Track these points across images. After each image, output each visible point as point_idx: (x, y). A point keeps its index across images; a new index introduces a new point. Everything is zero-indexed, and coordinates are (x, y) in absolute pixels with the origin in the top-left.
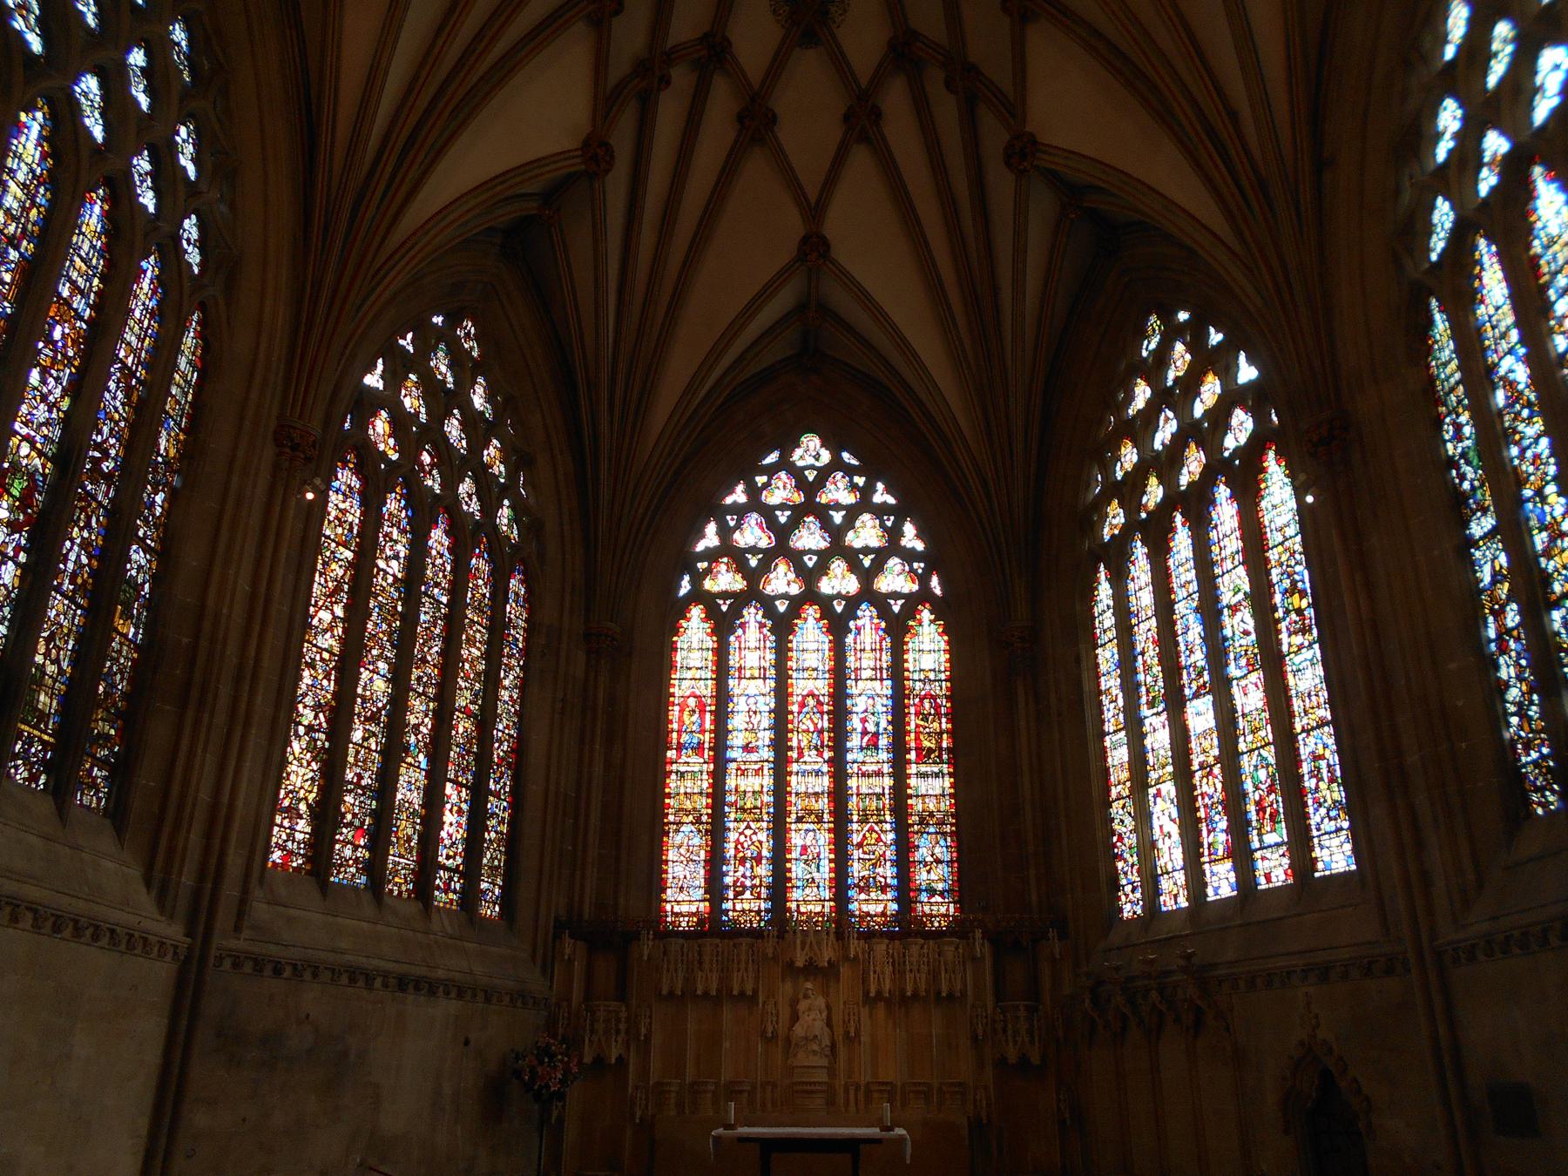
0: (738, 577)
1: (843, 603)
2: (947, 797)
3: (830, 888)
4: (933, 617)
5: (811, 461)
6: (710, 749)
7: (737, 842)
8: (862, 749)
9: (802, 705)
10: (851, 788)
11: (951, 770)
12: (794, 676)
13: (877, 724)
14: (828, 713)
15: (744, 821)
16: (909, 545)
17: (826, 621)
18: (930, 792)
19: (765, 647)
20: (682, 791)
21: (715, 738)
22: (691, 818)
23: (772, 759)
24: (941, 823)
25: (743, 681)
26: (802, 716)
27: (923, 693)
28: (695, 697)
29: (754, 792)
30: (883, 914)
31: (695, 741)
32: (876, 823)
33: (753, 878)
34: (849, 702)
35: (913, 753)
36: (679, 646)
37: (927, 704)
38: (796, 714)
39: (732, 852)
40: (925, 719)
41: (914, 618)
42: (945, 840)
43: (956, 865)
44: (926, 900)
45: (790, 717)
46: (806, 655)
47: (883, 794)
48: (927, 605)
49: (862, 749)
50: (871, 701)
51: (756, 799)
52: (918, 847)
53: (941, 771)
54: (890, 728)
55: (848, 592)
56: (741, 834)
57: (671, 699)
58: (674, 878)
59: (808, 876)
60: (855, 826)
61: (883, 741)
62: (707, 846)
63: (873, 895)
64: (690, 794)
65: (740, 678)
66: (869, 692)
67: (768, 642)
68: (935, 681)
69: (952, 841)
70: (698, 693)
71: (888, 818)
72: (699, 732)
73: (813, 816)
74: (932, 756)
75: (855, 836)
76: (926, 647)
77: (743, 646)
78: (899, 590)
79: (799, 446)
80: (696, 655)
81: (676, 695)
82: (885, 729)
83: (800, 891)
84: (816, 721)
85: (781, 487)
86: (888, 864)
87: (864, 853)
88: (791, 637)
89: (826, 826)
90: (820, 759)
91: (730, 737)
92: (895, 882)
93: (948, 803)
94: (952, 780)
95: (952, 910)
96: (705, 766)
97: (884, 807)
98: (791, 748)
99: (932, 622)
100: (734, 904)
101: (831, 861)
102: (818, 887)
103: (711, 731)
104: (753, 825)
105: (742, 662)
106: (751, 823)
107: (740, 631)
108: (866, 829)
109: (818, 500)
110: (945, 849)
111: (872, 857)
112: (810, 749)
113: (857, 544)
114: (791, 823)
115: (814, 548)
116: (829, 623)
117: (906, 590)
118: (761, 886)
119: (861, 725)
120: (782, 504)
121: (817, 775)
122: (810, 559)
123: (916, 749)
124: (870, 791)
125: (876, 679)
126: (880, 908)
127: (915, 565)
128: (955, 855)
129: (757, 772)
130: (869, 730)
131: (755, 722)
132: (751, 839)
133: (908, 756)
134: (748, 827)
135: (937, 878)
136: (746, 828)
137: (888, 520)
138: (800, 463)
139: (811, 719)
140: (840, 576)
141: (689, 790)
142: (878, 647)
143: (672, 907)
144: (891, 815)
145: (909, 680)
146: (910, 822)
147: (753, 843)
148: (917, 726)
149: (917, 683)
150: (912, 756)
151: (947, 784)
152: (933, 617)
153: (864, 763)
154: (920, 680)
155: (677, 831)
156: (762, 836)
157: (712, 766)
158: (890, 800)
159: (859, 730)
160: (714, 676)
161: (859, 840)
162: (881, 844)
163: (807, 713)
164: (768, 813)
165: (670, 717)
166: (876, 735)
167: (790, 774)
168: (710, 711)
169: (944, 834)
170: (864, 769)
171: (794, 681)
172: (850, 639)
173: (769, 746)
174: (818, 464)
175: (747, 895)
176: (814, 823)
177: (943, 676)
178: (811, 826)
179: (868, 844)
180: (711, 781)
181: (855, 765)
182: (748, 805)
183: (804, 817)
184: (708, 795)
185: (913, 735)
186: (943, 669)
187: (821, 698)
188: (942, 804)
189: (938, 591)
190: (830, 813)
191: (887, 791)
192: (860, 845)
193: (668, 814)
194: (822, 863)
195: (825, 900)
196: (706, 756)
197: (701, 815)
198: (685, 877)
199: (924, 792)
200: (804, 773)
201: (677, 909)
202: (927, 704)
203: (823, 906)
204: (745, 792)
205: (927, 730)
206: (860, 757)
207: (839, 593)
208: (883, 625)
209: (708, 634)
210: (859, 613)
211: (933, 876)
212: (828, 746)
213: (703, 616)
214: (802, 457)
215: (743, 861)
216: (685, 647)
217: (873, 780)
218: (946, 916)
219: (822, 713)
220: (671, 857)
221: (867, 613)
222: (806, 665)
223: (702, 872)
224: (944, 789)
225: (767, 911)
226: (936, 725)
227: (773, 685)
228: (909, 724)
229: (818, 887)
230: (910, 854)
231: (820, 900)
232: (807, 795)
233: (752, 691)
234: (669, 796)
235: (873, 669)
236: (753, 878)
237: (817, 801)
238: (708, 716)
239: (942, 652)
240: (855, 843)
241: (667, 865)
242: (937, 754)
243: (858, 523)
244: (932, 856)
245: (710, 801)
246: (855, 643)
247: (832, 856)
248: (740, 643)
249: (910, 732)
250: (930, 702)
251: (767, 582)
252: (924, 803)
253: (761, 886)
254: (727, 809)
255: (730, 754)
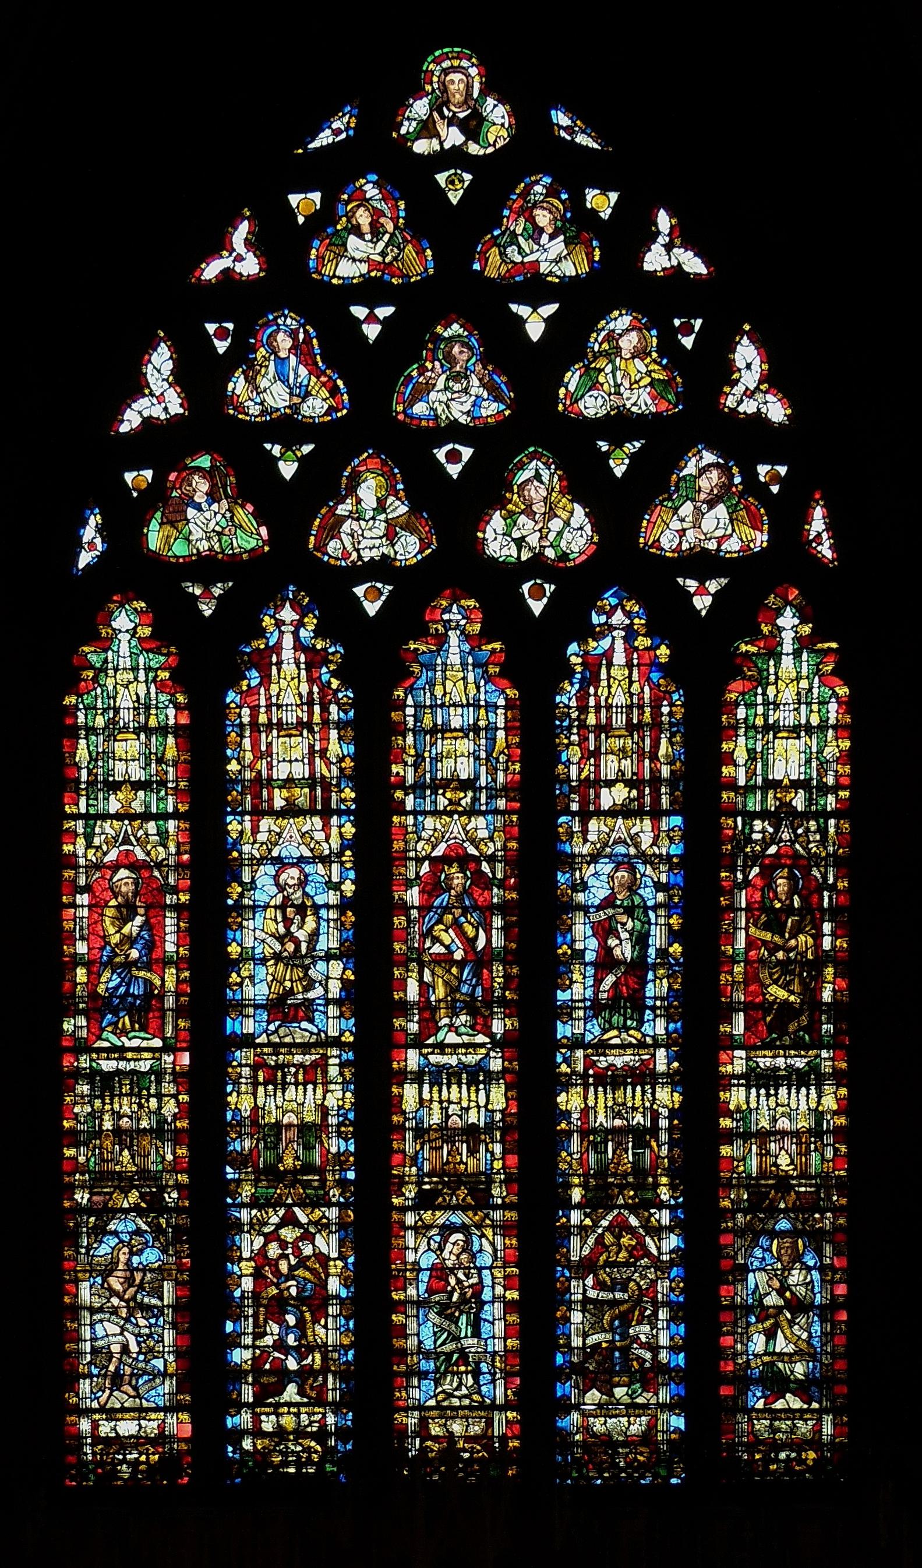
0: (244, 515)
1: (550, 588)
2: (829, 1139)
3: (507, 1376)
4: (806, 630)
5: (454, 137)
6: (179, 1012)
7: (261, 1257)
8: (596, 1008)
9: (433, 887)
10: (568, 1113)
11: (844, 1065)
12: (409, 806)
13: (641, 940)
14: (503, 908)
15: (278, 1203)
16: (749, 407)
17: (497, 646)
18: (783, 1124)
19: (325, 723)
20: (108, 1125)
21: (191, 981)
22: (134, 1197)
23: (348, 1038)
24: (807, 1206)
25: (265, 823)
26: (431, 917)
27: (773, 850)
28: (134, 866)
29: (304, 1128)
30: (647, 1437)
31: (137, 990)
32: (633, 1209)
33: (303, 1350)
34: (562, 878)
35: (740, 1019)
36: (81, 718)
37: (782, 885)
38: (415, 913)
39: (248, 1284)
40: (775, 924)
41: (754, 635)
42: (819, 1253)
43: (844, 1316)
44: (760, 1405)
45: (399, 921)
46: (443, 746)
47: (654, 1130)
48: (793, 594)
49: (596, 1008)
50: (622, 874)
51: (308, 1148)
52: (745, 1270)
53: (813, 1068)
54: (676, 948)
55: (564, 557)
56: (269, 1238)
57: (68, 874)
58: (95, 1351)
59: (449, 1347)
60: (575, 1217)
61: (656, 988)
62: (181, 1269)
63: (619, 1392)
64: (129, 1132)
65: (257, 813)
66: (621, 849)
67: (333, 708)
68: (806, 815)
69: (836, 1253)
70: (140, 854)
71: (665, 1194)
72: (148, 967)
73: (462, 1192)
74: (791, 1028)
75: (575, 1242)
76: (786, 717)
77: (263, 719)
78: (712, 545)
79: (418, 93)
80: (129, 746)
81: (82, 861)
82: (662, 953)
83: (428, 1385)
84: (470, 931)
85: (366, 228)
86: (662, 1314)
87: (599, 1285)
88: (400, 693)
89: (497, 1215)
90: (481, 1039)
91: (234, 977)
92: (681, 1359)
93: (829, 1153)
94: (843, 1091)
95: (827, 1429)
96: (169, 1059)
97: (655, 1166)
98: (404, 1008)
99: (803, 644)
100: (256, 1419)
101: (509, 1306)
102: (477, 1373)
103: (178, 963)
104: (302, 1216)
105: (262, 765)
106: (296, 1210)
107: (254, 677)
108: (605, 1223)
109: (477, 266)
110: (816, 1275)
111: (618, 1295)
112: (454, 1013)
113: (592, 406)
114: (403, 1209)
115: (463, 419)
116: (508, 651)
117: (733, 546)
118: (325, 1370)
119: (593, 943)
120: (367, 281)
121: (473, 1082)
122: (454, 457)
123: (747, 1008)
124: (618, 1122)
125: (640, 813)
126: (638, 1426)
127: (763, 470)
128: (841, 1290)
129: (315, 1073)
130: (617, 952)
131: (301, 935)
132: (297, 1252)
133: (725, 1028)
134: (289, 1220)
135: (790, 1349)
136: (283, 1223)
137: (687, 330)
138: (421, 147)
139: (457, 926)
140: (539, 508)
141: (125, 1122)
142: (647, 717)
143: (95, 1425)
144: (672, 1186)
145: (733, 813)
146: (726, 1204)
147: (303, 1262)
148: (751, 943)
149: (758, 825)
150: (739, 1025)
151: (829, 1102)
152: (806, 630)
153: (602, 1047)
154: (764, 815)
155: (100, 1232)
156: (327, 1244)
157: (185, 1059)
158: (672, 1144)
159: (590, 956)
160: (183, 808)
161: (586, 1251)
162: (644, 1262)
163: (447, 909)
164: (342, 1183)
165: (68, 925)
166: (638, 968)
167: (402, 1077)
168: (177, 908)
169: (816, 1239)
170: (603, 1062)
171: (410, 820)
172: (567, 696)
173: (338, 1002)
174: (473, 149)
175: (291, 1393)
176: (464, 1208)
177: (831, 802)
178: (457, 1218)
179: (607, 1264)
180: (184, 1098)
181: (580, 1053)
182: (289, 1161)
183: (435, 1193)
184: (177, 1137)
185: (738, 969)
186: (830, 780)
187: (485, 867)
188: (815, 1158)
189: (826, 550)
190: (506, 1182)
191: (664, 1123)
192: (587, 1266)
193: (71, 1188)
194: (486, 1314)
195: (494, 1407)
196: (169, 1031)
197: (162, 1189)
198: (125, 1349)
199: (765, 1124)
200: (438, 1076)
201: (105, 1429)
202: (782, 885)
203: (490, 1423)
204: (278, 1126)
205: (780, 955)
206: (594, 1031)
207: (538, 557)
208: (663, 652)
209: (161, 687)
210: (596, 619)
211: (781, 1344)
212: (503, 1002)
213: (147, 631)
214: (427, 129)
215: (277, 1307)
216: (100, 722)
217: (634, 1096)
218: (815, 1442)
219: (487, 911)
220: (85, 1293)
221: (618, 618)
222: (445, 769)
223: (169, 1336)
224: (819, 1115)
225: (341, 1433)
226: (804, 940)
227: (349, 830)
228: (732, 940)
229: (477, 1373)
230: (724, 1290)
231: (482, 1406)
232: (446, 1133)
233: (291, 850)
234: (74, 1138)
235: (630, 784)
236: (303, 1350)
237: (473, 1151)
238: (170, 921)
239: (830, 733)
240: (574, 1258)
241: (76, 1318)
242: (804, 1020)
243: (596, 342)
244: (781, 1292)
245: (182, 1151)
246: (583, 709)
247: (513, 1295)
248: (255, 710)
249: (733, 960)
250: (791, 878)
251: (333, 528)
252: (762, 1155)
253: (325, 1370)
254: (230, 1173)
255: (231, 1026)
